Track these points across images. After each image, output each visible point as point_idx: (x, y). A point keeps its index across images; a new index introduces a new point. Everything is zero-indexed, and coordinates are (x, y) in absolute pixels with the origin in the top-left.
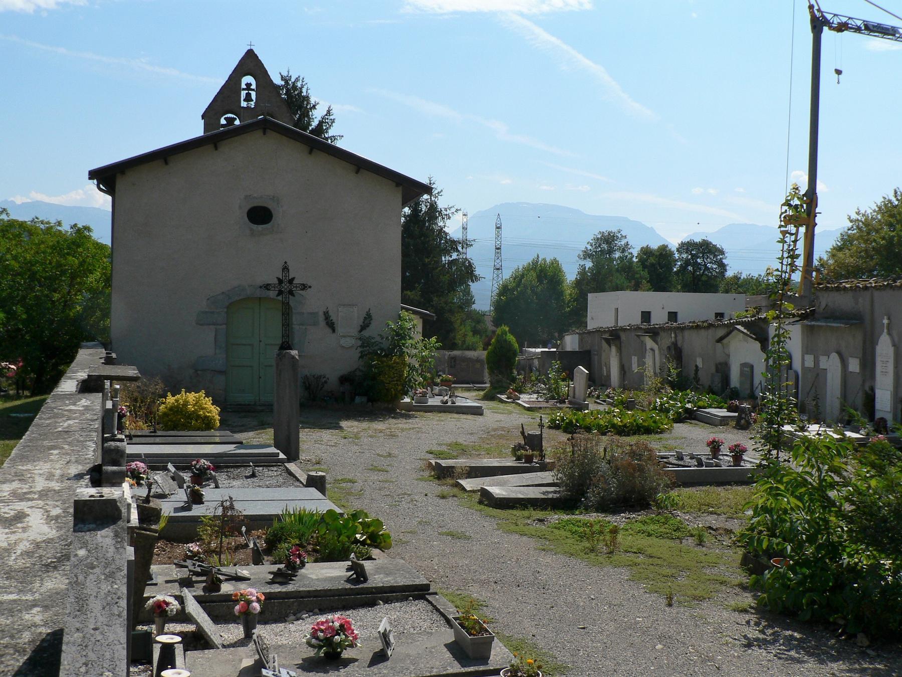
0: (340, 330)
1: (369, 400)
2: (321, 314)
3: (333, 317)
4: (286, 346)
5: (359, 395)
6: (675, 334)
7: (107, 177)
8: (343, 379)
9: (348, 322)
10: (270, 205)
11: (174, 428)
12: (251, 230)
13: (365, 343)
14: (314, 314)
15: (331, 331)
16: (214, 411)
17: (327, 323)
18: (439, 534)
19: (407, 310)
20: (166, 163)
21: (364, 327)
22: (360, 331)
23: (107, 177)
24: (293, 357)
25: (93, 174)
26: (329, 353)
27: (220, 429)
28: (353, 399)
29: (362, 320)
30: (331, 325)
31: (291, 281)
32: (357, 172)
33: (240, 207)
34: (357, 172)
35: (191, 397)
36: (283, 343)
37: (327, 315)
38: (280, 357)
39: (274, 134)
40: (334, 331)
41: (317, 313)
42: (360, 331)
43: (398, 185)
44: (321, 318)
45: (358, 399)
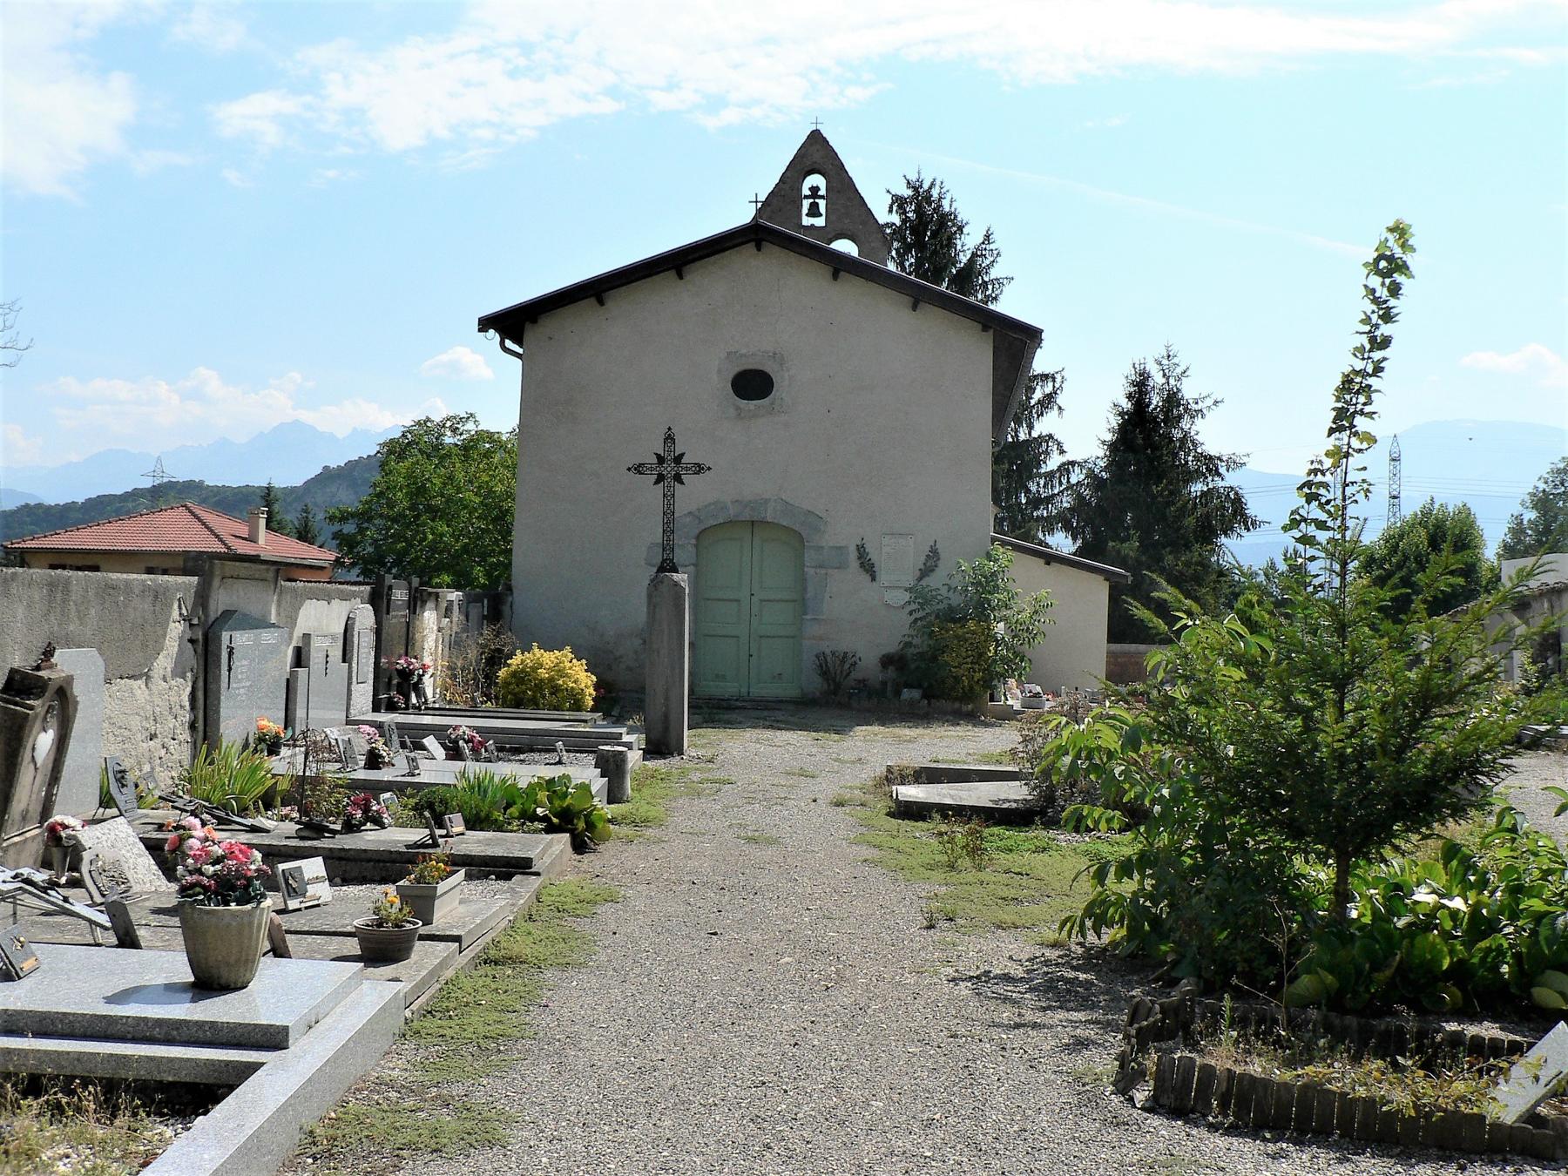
0: (884, 577)
1: (924, 696)
2: (853, 548)
3: (873, 556)
4: (668, 566)
5: (910, 686)
6: (1550, 601)
7: (510, 324)
8: (887, 661)
9: (899, 565)
10: (769, 367)
11: (518, 704)
12: (738, 408)
13: (920, 596)
14: (840, 549)
15: (868, 578)
16: (582, 678)
17: (862, 565)
18: (771, 842)
19: (1004, 543)
20: (601, 303)
21: (926, 571)
22: (920, 579)
23: (510, 324)
24: (676, 584)
25: (486, 324)
26: (868, 619)
27: (593, 710)
28: (898, 693)
29: (923, 558)
30: (868, 567)
31: (678, 459)
32: (914, 308)
33: (719, 371)
34: (914, 308)
35: (548, 658)
36: (664, 561)
37: (861, 551)
38: (655, 583)
39: (776, 249)
40: (873, 579)
41: (846, 547)
42: (920, 579)
43: (985, 328)
44: (853, 555)
45: (907, 694)
